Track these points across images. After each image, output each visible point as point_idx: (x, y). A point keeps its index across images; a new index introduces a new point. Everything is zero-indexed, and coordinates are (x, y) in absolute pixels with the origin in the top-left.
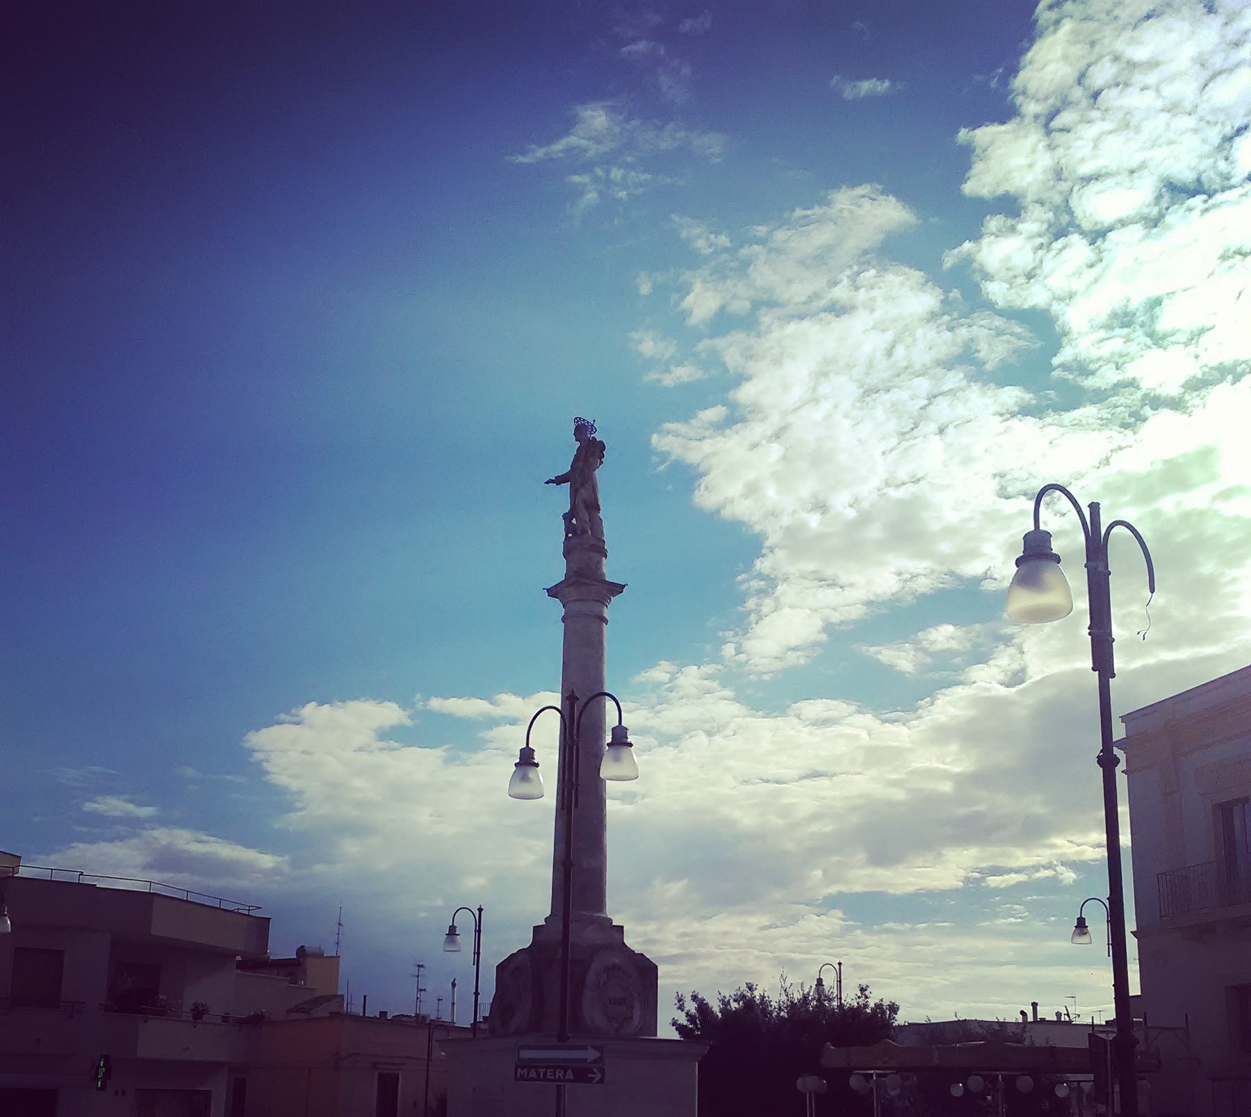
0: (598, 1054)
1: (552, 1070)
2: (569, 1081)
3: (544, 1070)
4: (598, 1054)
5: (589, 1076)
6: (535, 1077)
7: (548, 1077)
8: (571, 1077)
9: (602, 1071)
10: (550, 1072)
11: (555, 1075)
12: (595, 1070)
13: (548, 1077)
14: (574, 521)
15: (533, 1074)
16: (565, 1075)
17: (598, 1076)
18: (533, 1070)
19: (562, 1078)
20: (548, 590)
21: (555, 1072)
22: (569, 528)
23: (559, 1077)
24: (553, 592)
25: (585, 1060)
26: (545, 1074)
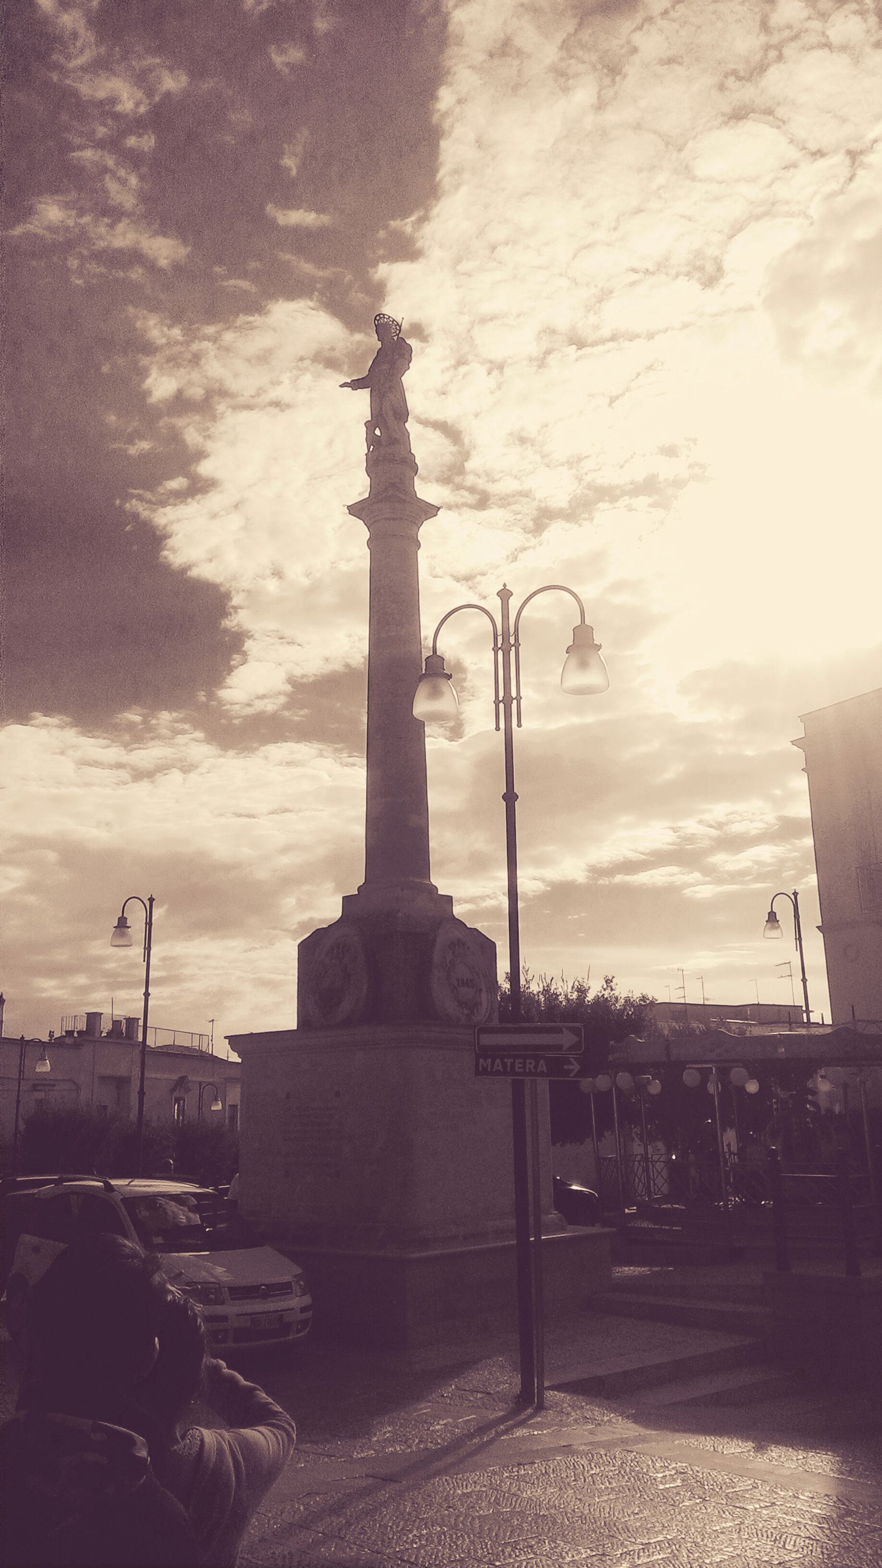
2: (542, 1074)
5: (565, 1067)
6: (502, 1070)
8: (545, 1071)
11: (524, 1067)
12: (572, 1060)
13: (517, 1069)
14: (378, 432)
15: (498, 1065)
16: (536, 1067)
18: (498, 1061)
19: (533, 1071)
20: (348, 507)
21: (524, 1064)
22: (371, 440)
23: (530, 1068)
24: (356, 510)
25: (559, 1047)
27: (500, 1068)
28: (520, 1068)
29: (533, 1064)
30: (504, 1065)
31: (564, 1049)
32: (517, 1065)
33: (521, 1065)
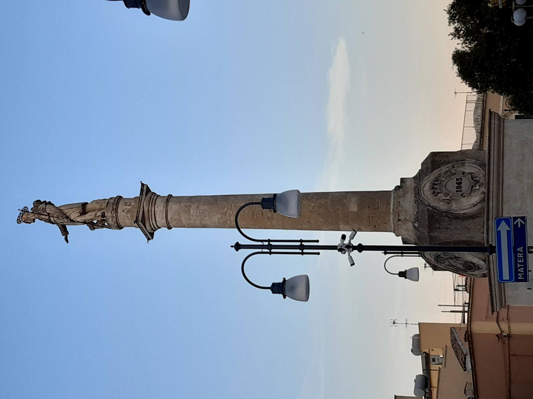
0: (503, 223)
1: (518, 259)
3: (518, 264)
4: (503, 223)
7: (523, 261)
9: (515, 219)
10: (519, 260)
12: (515, 223)
13: (523, 261)
17: (519, 220)
26: (520, 263)
27: (522, 269)
28: (522, 260)
29: (519, 254)
30: (520, 267)
31: (509, 229)
32: (520, 261)
33: (520, 260)
